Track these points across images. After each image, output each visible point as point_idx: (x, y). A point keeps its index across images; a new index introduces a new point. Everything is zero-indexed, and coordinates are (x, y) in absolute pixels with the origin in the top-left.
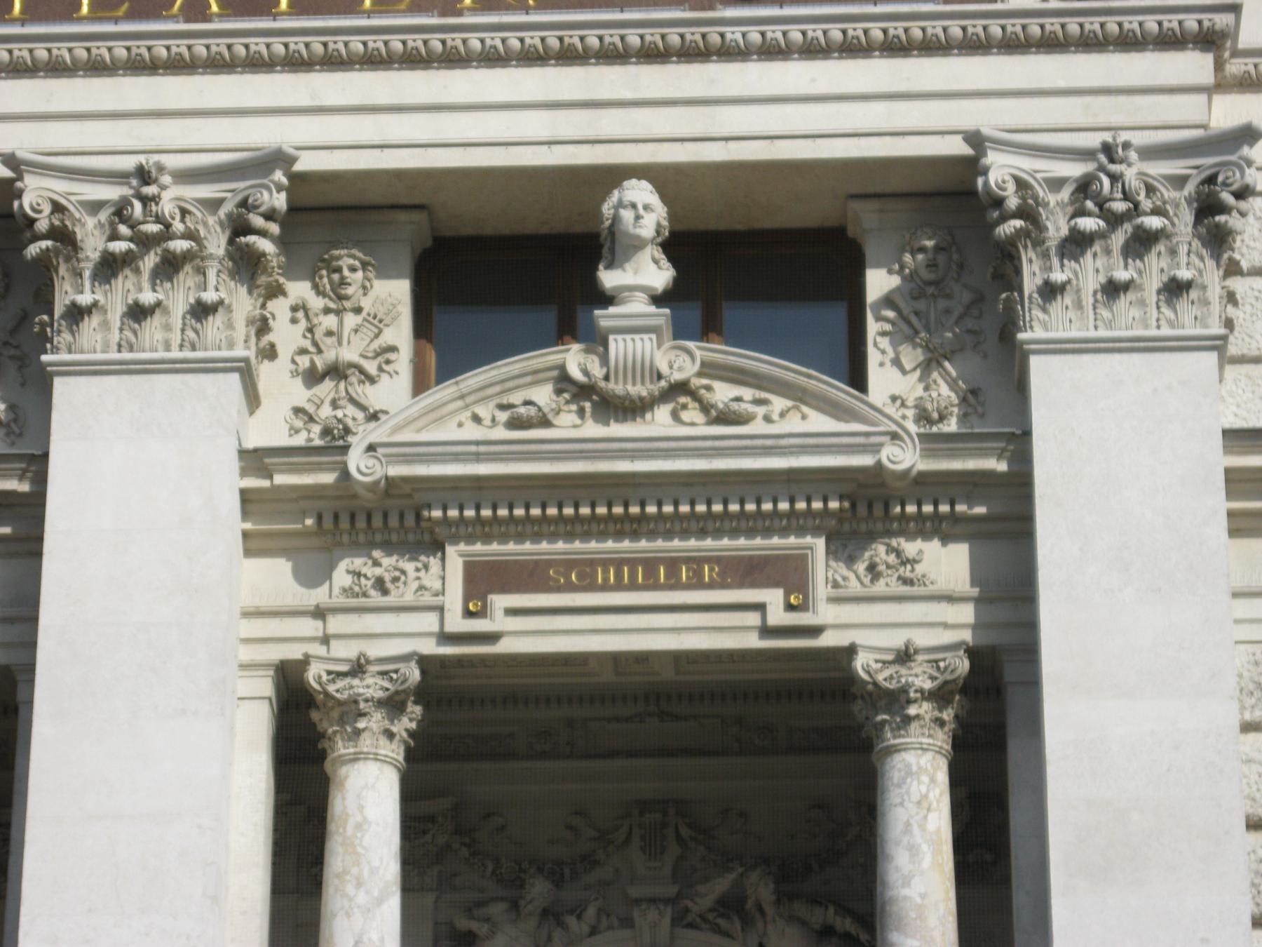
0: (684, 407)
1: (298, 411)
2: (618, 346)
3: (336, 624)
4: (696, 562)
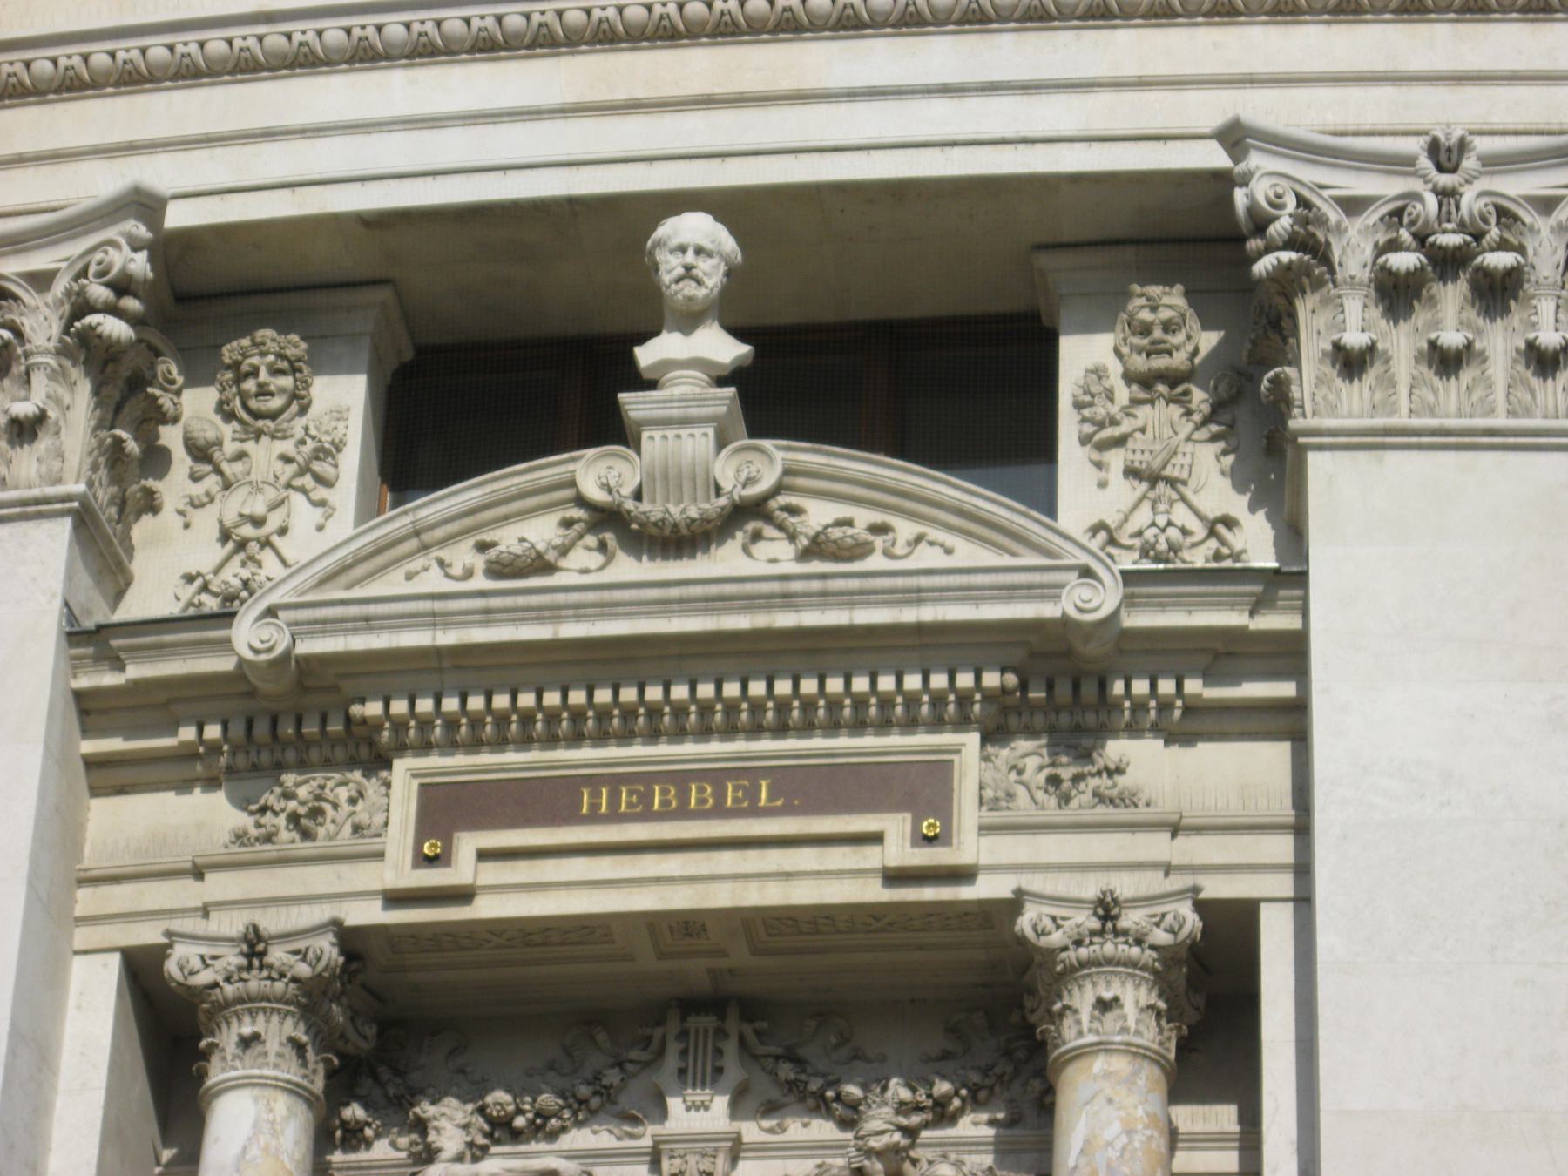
3: (219, 886)
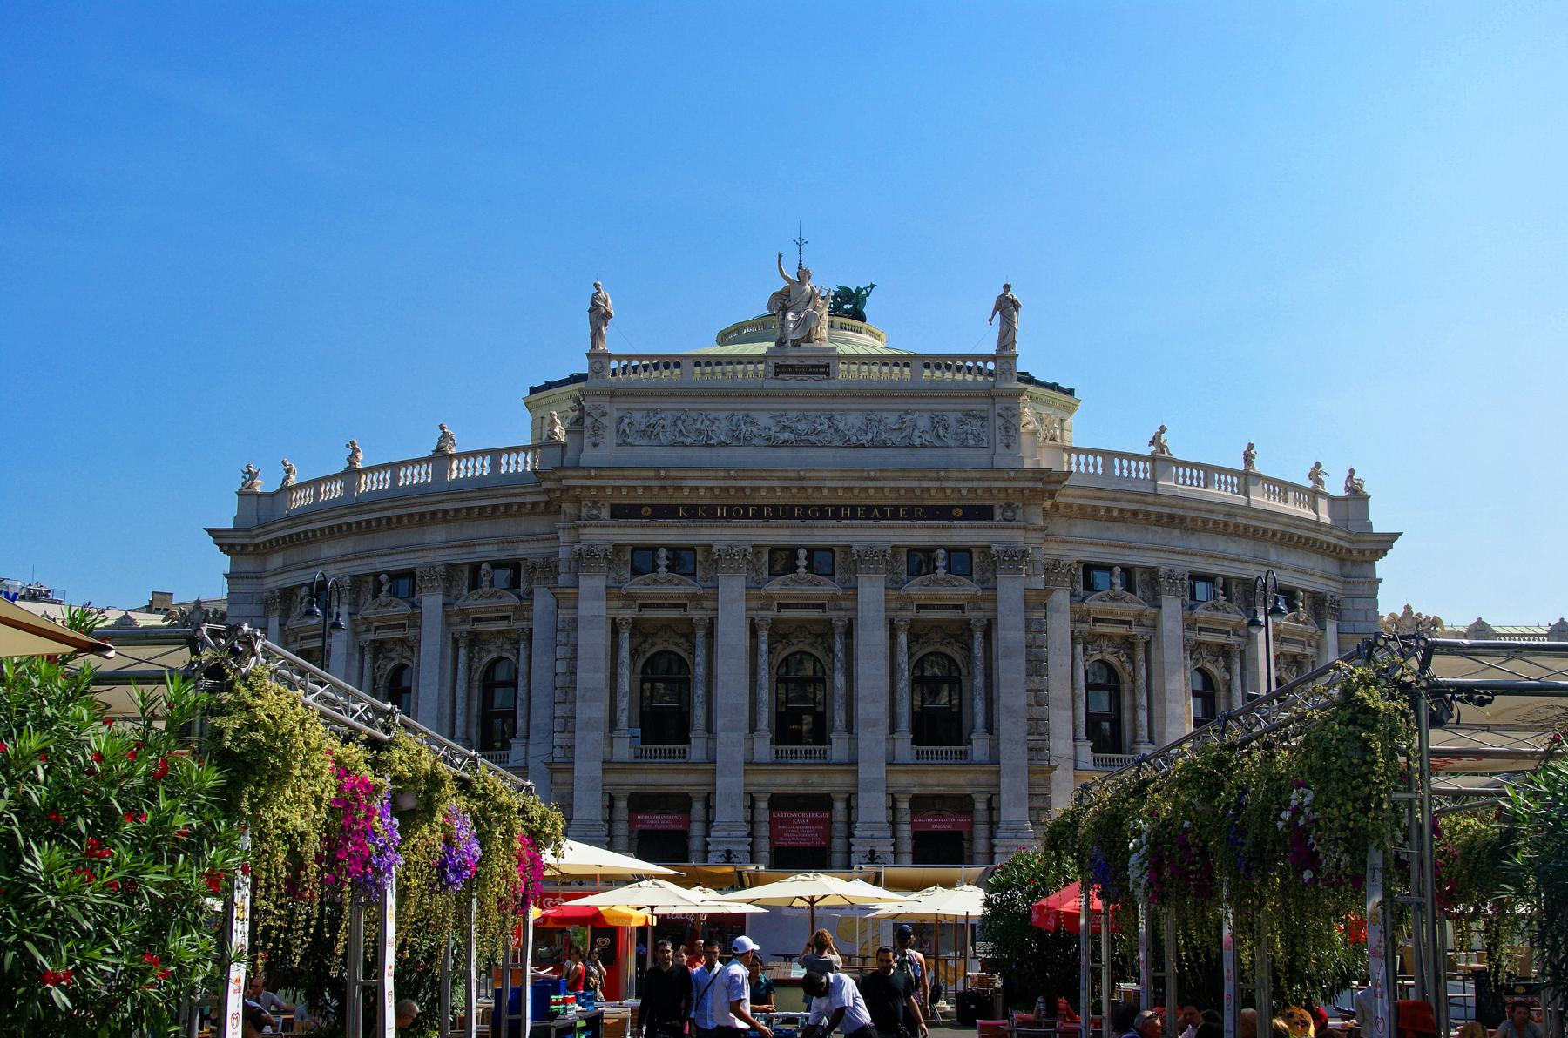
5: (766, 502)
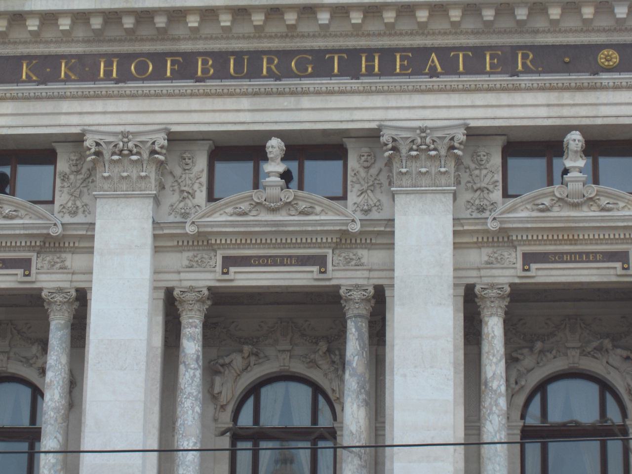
0: (592, 205)
1: (468, 202)
2: (570, 185)
3: (483, 272)
4: (595, 253)
5: (200, 46)
